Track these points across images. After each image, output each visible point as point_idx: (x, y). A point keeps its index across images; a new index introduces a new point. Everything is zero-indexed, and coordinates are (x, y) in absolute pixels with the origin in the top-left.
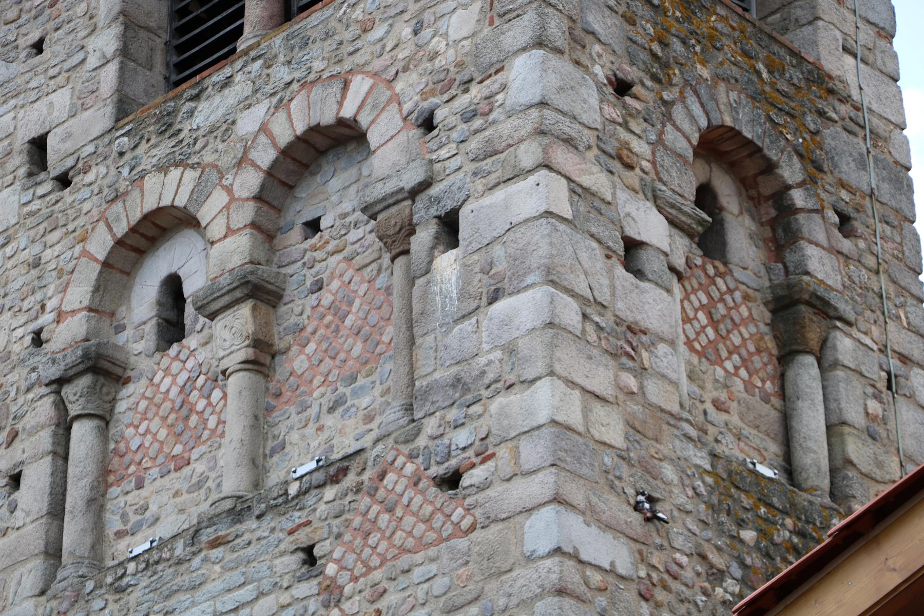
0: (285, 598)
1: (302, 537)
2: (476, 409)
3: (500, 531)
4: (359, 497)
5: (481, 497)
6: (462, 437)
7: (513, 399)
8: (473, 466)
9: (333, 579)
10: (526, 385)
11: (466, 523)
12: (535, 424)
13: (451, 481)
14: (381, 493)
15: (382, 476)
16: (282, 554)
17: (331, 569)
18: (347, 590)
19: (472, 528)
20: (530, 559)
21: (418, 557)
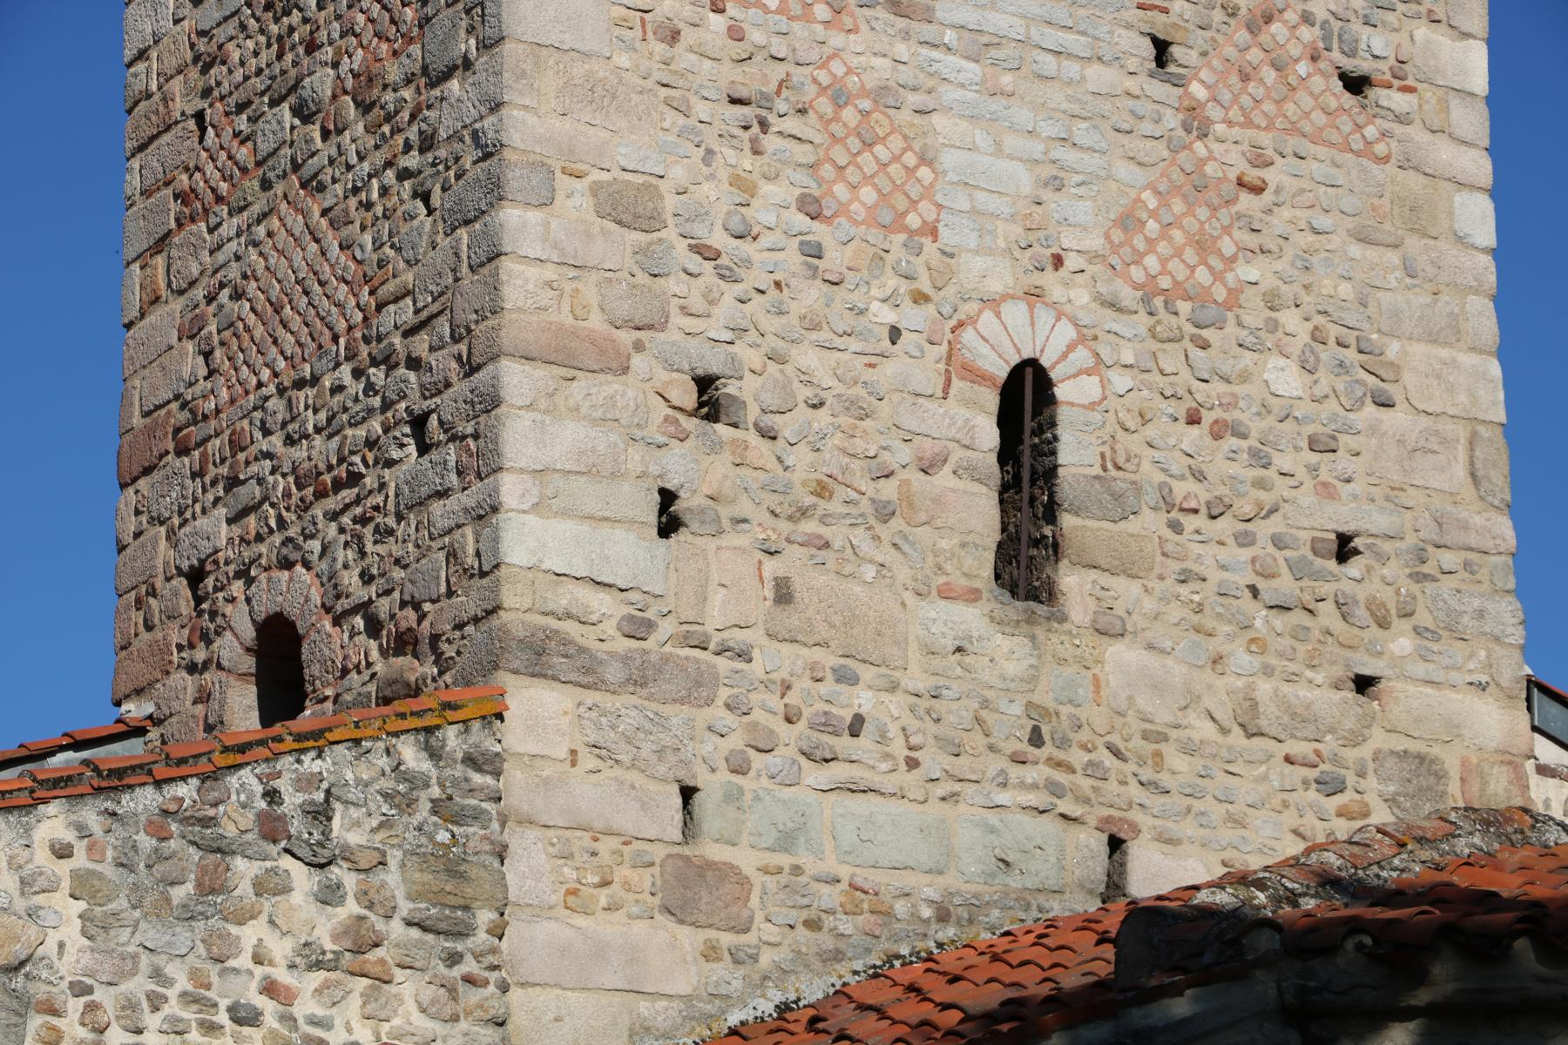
0: (1131, 84)
1: (1160, 25)
2: (1390, 17)
3: (1425, 187)
4: (1232, 22)
5: (1398, 129)
6: (1379, 42)
7: (1442, 40)
8: (1390, 87)
9: (1202, 105)
10: (1455, 33)
11: (1380, 149)
12: (1468, 89)
13: (1356, 84)
14: (1263, 38)
15: (1268, 19)
16: (1129, 26)
17: (1198, 90)
18: (1220, 128)
19: (1385, 160)
20: (1460, 240)
21: (1321, 151)
